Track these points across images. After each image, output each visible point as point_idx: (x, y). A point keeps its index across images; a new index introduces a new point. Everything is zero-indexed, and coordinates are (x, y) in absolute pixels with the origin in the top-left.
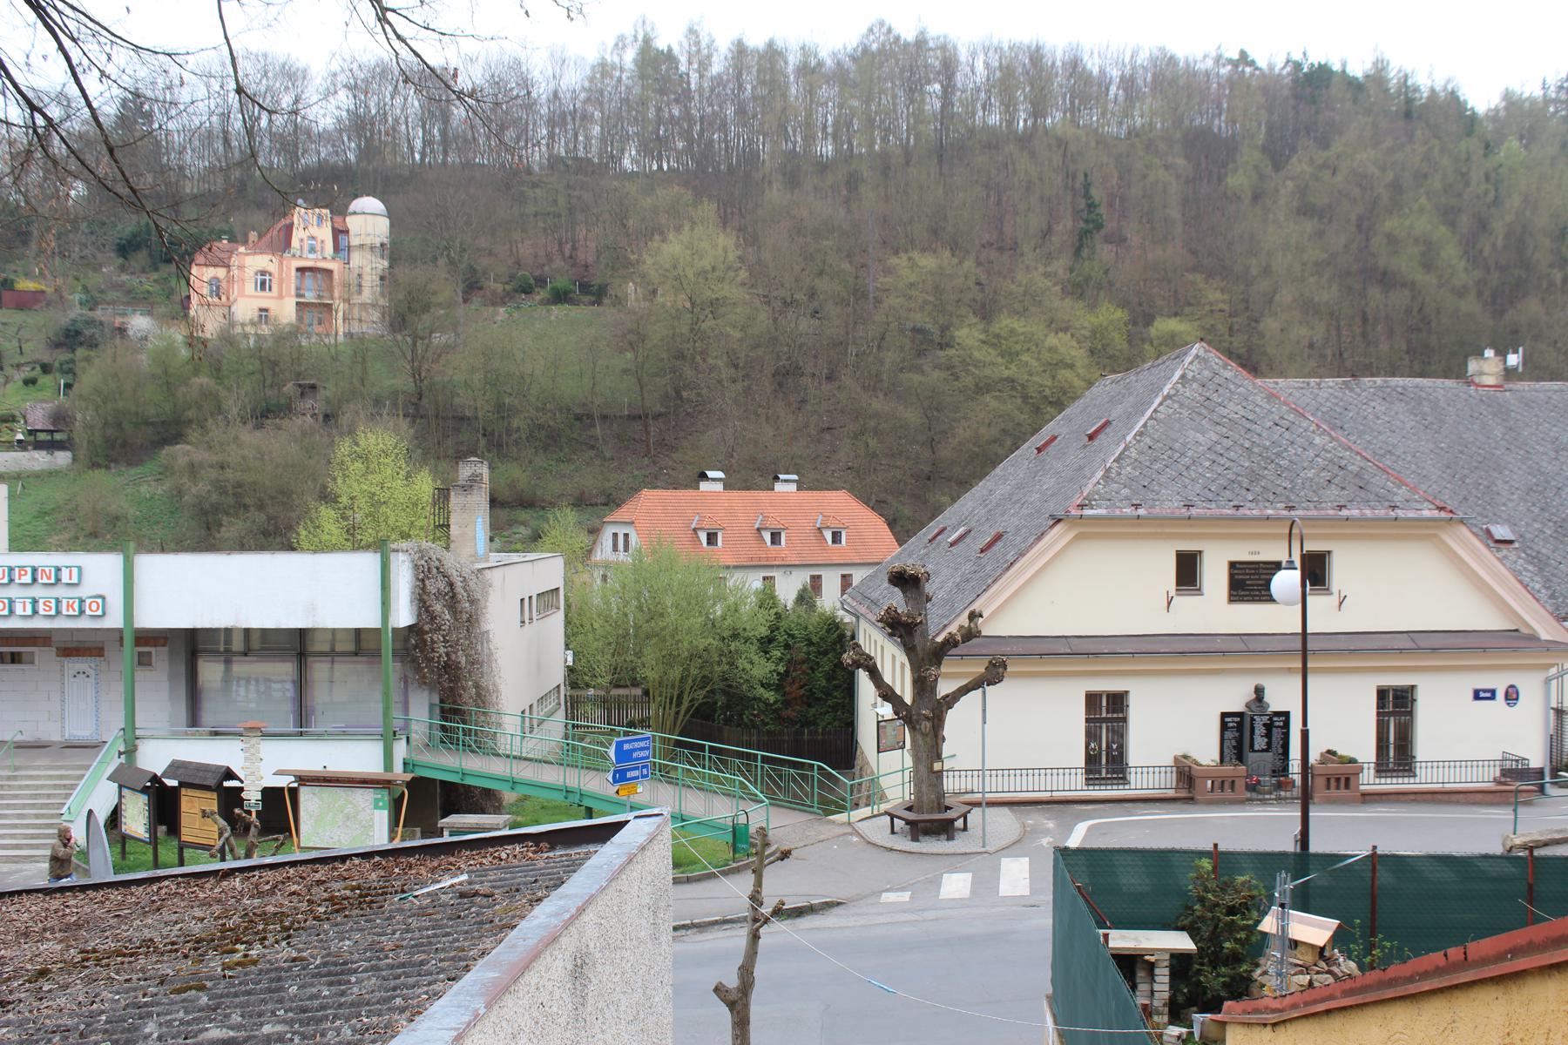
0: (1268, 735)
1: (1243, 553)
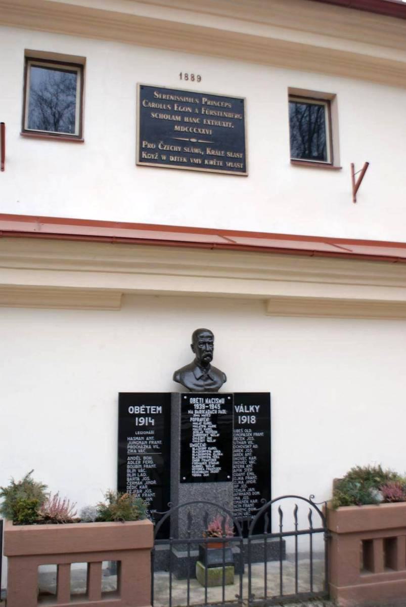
0: (224, 443)
1: (168, 72)
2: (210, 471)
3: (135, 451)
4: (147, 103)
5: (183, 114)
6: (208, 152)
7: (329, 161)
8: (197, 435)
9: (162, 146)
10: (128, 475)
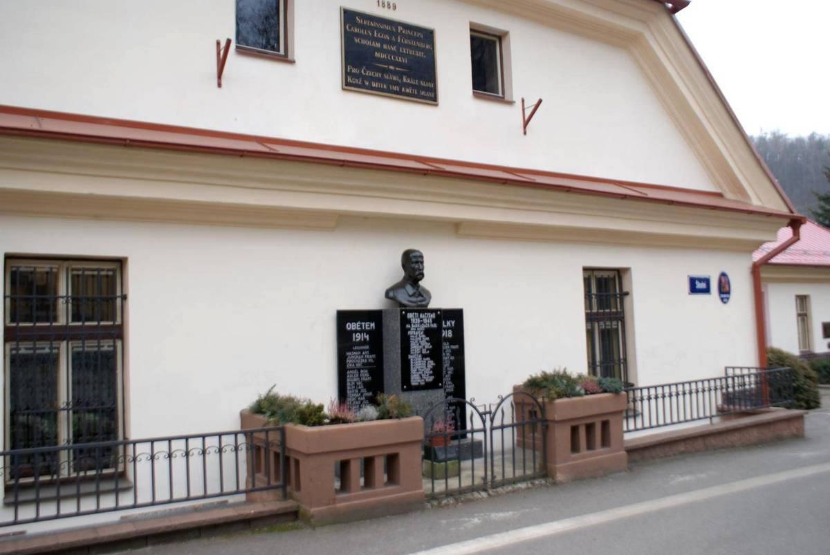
2: (425, 380)
3: (354, 365)
4: (350, 28)
5: (383, 41)
6: (404, 80)
7: (500, 95)
8: (414, 347)
9: (365, 72)
10: (348, 388)
